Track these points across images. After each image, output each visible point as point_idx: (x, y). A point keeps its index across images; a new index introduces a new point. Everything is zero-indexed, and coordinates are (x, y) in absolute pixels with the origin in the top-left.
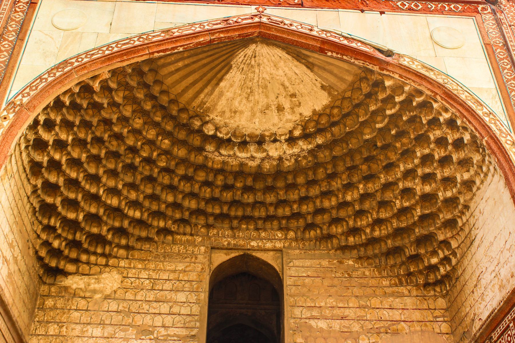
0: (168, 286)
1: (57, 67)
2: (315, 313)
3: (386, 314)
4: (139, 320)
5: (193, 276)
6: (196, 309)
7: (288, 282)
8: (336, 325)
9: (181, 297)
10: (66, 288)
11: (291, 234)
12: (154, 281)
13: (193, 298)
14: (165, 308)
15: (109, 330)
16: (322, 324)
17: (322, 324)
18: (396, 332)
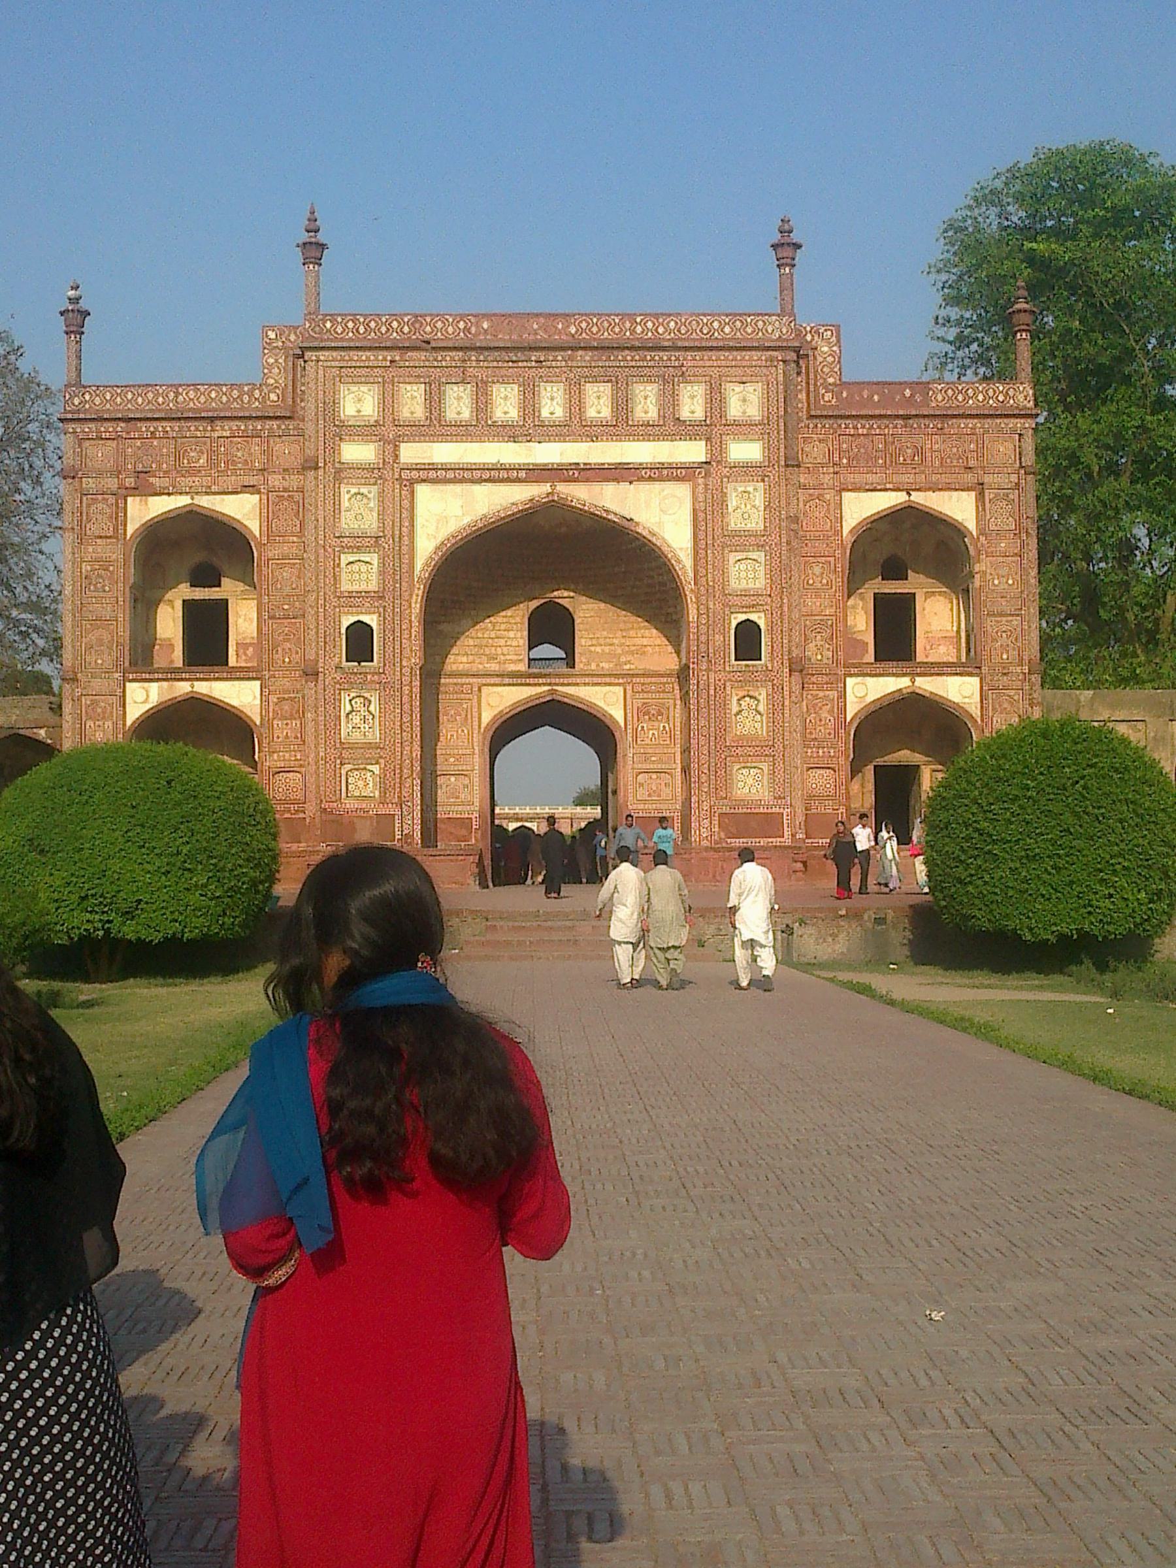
0: (503, 627)
1: (438, 548)
2: (594, 642)
3: (639, 641)
4: (487, 651)
5: (518, 619)
6: (521, 642)
7: (577, 621)
8: (607, 649)
9: (512, 634)
10: (441, 632)
11: (581, 586)
12: (494, 625)
13: (519, 635)
14: (502, 642)
15: (471, 658)
16: (598, 649)
17: (598, 649)
18: (644, 653)
